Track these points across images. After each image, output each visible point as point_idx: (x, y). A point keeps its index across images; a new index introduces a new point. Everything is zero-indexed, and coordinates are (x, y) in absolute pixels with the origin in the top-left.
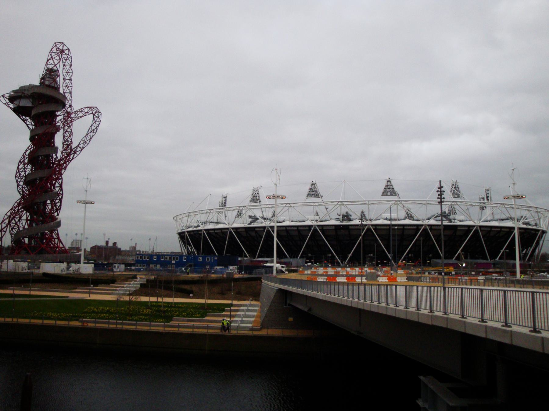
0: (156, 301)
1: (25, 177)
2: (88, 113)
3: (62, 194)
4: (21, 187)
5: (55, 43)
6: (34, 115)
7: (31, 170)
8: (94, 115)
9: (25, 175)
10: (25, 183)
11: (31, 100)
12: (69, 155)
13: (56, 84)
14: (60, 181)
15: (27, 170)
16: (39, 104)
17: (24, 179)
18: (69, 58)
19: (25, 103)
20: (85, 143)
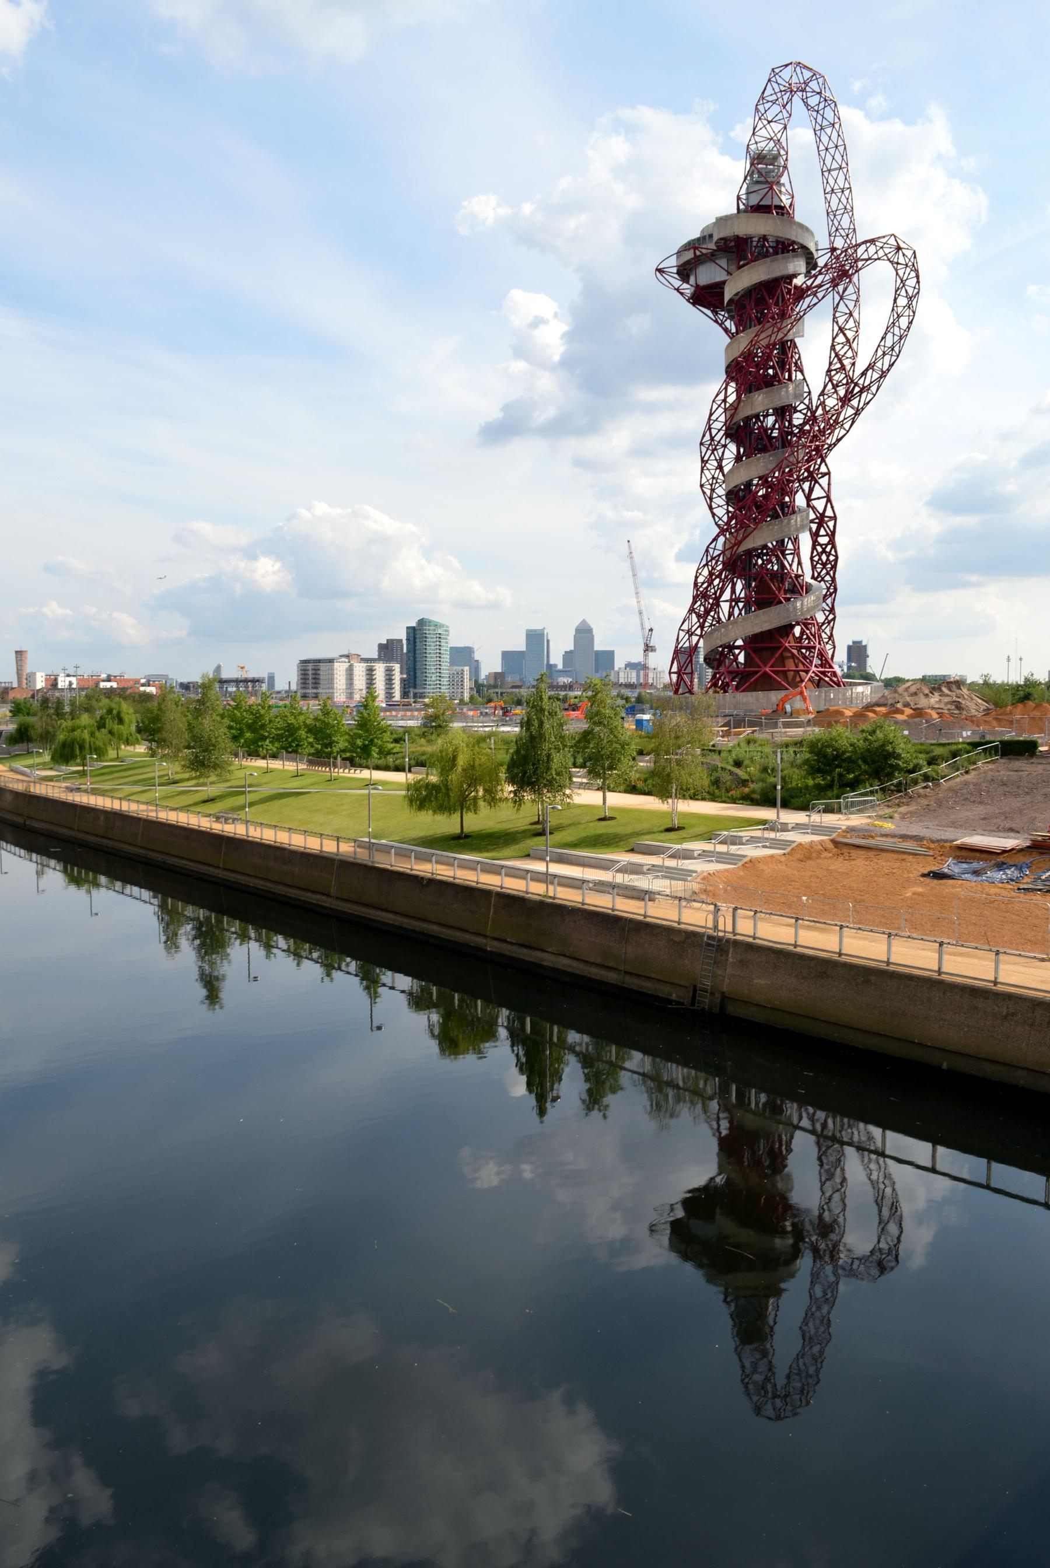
0: (458, 831)
1: (724, 482)
2: (870, 259)
3: (834, 518)
4: (720, 512)
5: (773, 70)
6: (731, 301)
7: (738, 458)
8: (895, 264)
9: (721, 477)
10: (732, 496)
11: (723, 262)
12: (845, 401)
13: (775, 197)
14: (824, 481)
15: (724, 463)
16: (740, 267)
17: (724, 486)
18: (830, 102)
19: (708, 274)
20: (892, 355)
